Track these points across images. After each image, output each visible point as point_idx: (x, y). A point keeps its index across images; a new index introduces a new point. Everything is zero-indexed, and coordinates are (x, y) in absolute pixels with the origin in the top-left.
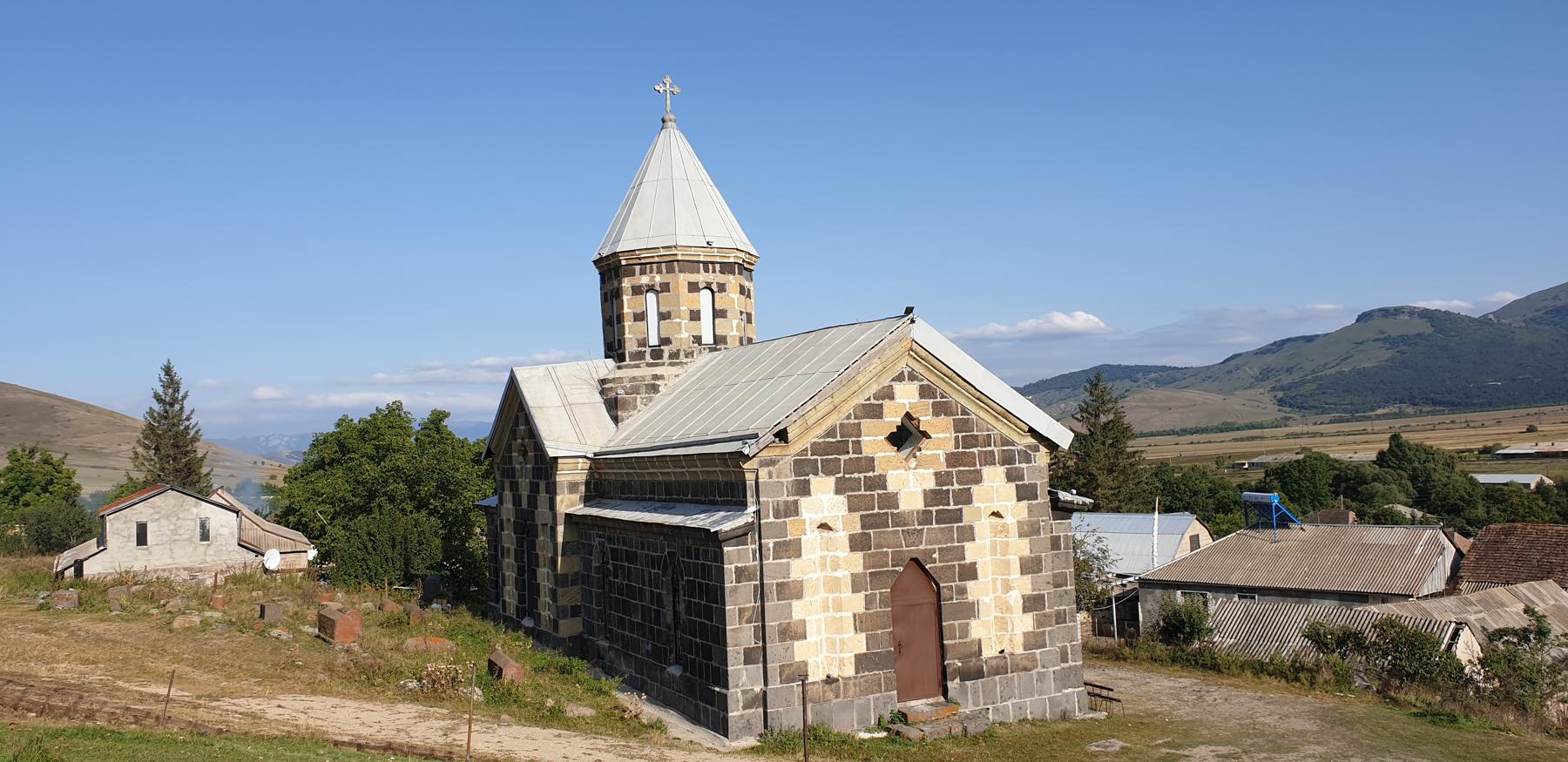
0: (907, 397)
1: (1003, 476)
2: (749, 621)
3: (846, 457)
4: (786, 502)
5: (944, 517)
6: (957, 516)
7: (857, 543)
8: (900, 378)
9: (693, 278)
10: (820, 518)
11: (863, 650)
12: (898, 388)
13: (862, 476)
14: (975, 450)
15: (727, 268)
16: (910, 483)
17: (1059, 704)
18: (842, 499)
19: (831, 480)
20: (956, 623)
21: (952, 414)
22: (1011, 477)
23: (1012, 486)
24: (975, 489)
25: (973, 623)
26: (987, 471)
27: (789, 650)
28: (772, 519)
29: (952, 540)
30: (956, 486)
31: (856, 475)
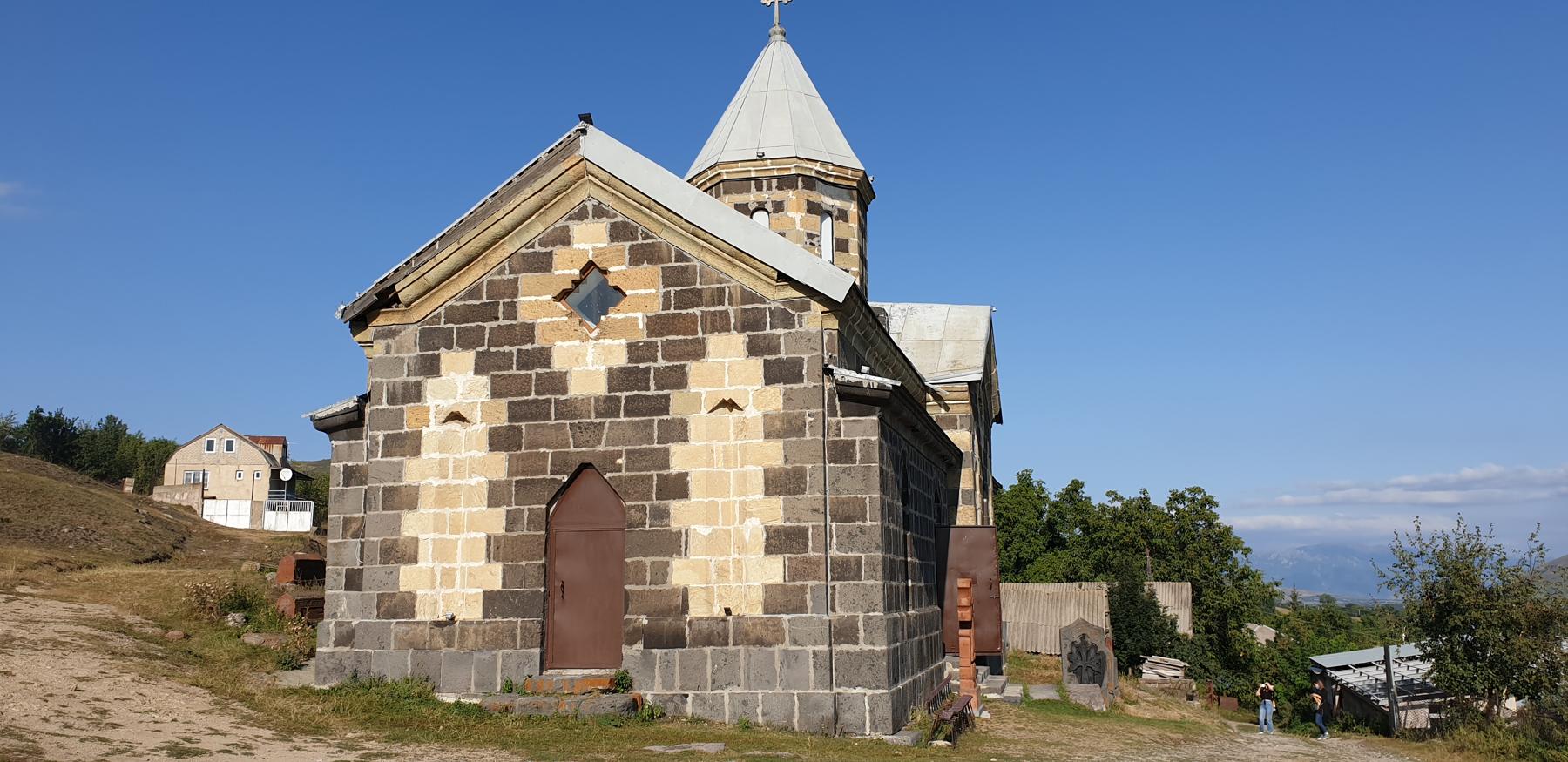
0: (590, 239)
1: (742, 347)
2: (355, 536)
3: (494, 324)
4: (405, 384)
5: (634, 407)
6: (662, 405)
7: (499, 440)
8: (581, 215)
9: (741, 198)
10: (449, 405)
11: (498, 586)
12: (577, 229)
13: (514, 349)
14: (697, 311)
15: (787, 182)
16: (587, 361)
17: (818, 706)
18: (485, 380)
19: (470, 356)
20: (648, 561)
21: (660, 260)
22: (753, 349)
23: (757, 363)
24: (692, 367)
25: (676, 563)
26: (714, 341)
27: (393, 577)
28: (384, 405)
29: (650, 440)
30: (661, 363)
31: (506, 349)
